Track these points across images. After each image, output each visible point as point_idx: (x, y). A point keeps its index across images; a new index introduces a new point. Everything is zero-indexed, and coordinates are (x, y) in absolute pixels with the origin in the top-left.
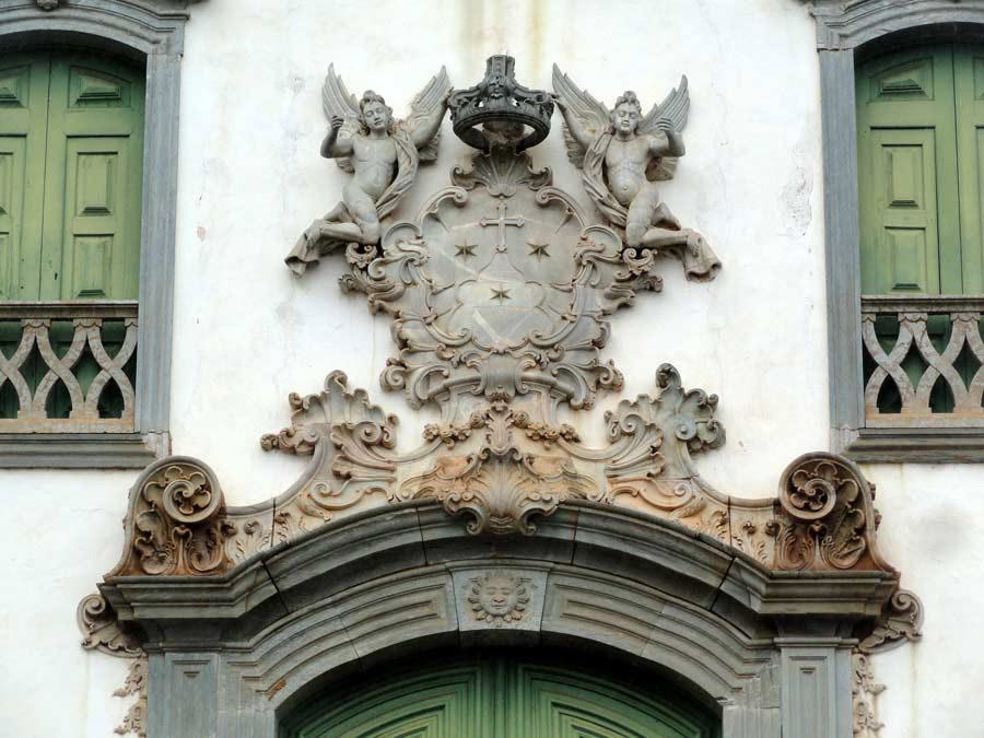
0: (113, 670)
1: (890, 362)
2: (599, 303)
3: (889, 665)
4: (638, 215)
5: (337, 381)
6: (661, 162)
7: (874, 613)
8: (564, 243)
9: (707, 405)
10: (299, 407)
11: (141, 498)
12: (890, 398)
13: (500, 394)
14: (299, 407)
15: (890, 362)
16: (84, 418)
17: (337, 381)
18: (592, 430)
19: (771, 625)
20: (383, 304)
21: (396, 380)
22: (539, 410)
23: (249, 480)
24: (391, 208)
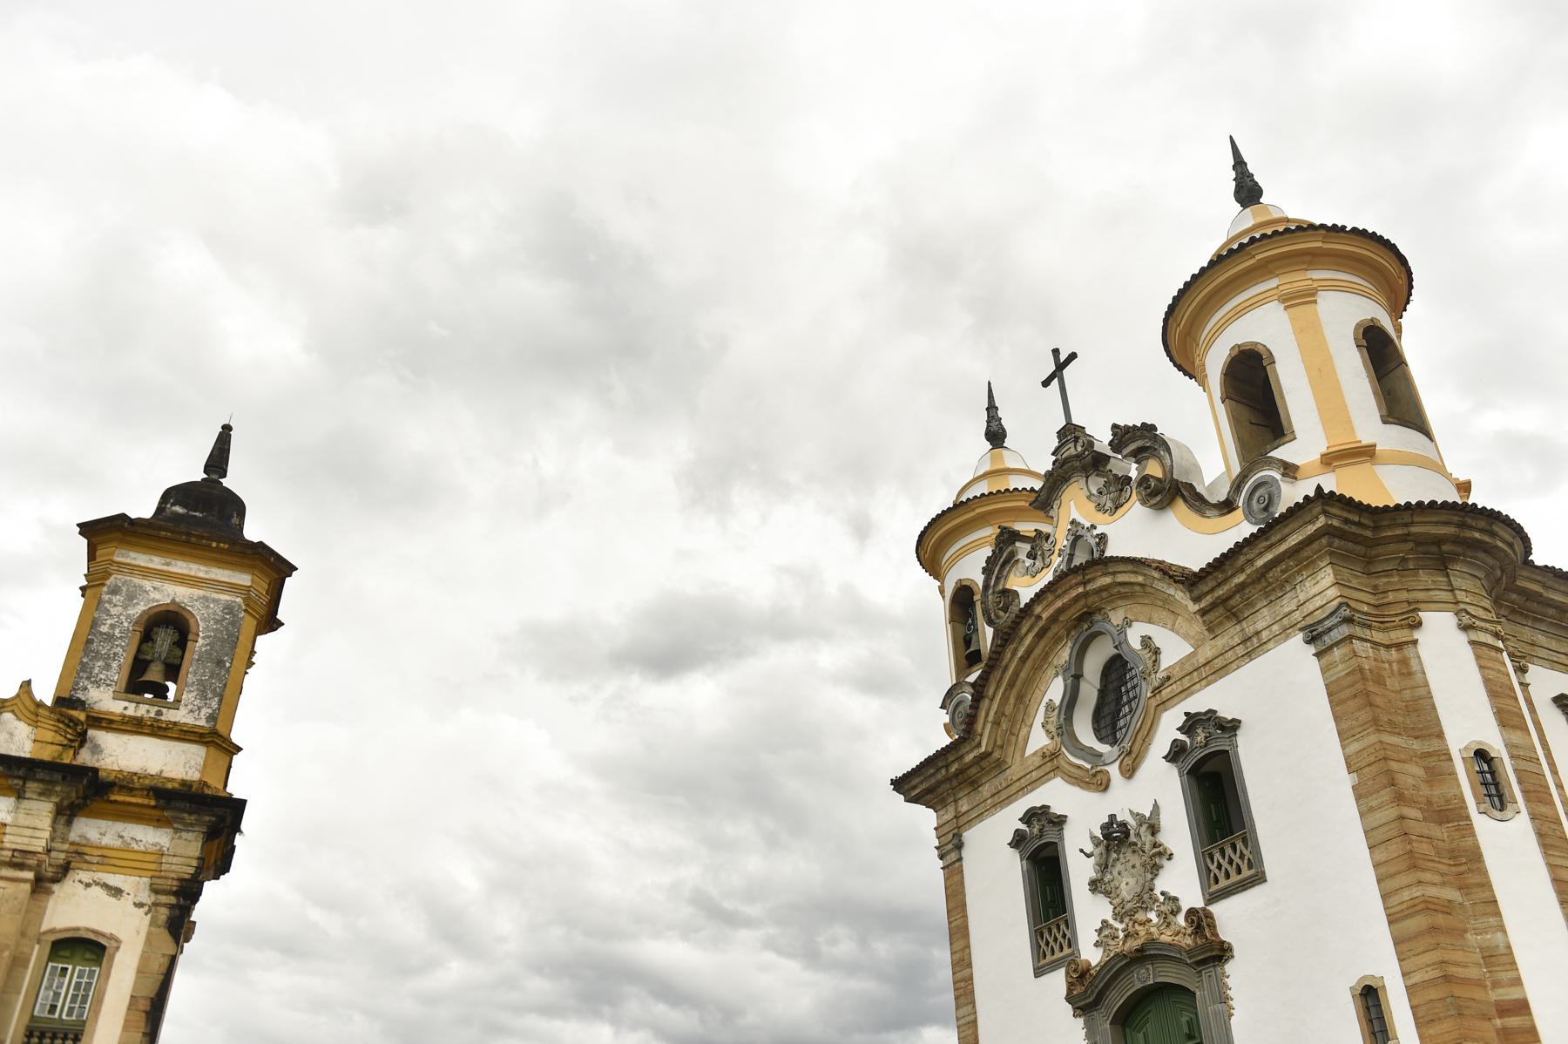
0: (1080, 1021)
1: (1213, 867)
2: (1149, 876)
3: (1229, 968)
4: (1147, 847)
5: (1104, 922)
6: (1154, 829)
7: (1219, 953)
8: (1136, 860)
9: (1175, 899)
10: (1100, 931)
11: (1067, 973)
12: (1217, 881)
13: (1131, 913)
14: (1100, 931)
15: (1213, 867)
16: (1067, 951)
17: (1104, 922)
18: (1152, 916)
19: (1199, 963)
20: (1107, 894)
21: (1116, 916)
22: (1140, 916)
23: (1091, 955)
24: (1104, 867)
